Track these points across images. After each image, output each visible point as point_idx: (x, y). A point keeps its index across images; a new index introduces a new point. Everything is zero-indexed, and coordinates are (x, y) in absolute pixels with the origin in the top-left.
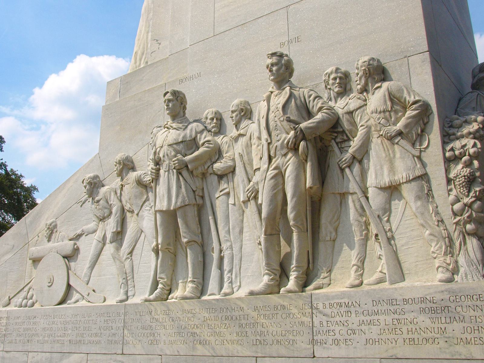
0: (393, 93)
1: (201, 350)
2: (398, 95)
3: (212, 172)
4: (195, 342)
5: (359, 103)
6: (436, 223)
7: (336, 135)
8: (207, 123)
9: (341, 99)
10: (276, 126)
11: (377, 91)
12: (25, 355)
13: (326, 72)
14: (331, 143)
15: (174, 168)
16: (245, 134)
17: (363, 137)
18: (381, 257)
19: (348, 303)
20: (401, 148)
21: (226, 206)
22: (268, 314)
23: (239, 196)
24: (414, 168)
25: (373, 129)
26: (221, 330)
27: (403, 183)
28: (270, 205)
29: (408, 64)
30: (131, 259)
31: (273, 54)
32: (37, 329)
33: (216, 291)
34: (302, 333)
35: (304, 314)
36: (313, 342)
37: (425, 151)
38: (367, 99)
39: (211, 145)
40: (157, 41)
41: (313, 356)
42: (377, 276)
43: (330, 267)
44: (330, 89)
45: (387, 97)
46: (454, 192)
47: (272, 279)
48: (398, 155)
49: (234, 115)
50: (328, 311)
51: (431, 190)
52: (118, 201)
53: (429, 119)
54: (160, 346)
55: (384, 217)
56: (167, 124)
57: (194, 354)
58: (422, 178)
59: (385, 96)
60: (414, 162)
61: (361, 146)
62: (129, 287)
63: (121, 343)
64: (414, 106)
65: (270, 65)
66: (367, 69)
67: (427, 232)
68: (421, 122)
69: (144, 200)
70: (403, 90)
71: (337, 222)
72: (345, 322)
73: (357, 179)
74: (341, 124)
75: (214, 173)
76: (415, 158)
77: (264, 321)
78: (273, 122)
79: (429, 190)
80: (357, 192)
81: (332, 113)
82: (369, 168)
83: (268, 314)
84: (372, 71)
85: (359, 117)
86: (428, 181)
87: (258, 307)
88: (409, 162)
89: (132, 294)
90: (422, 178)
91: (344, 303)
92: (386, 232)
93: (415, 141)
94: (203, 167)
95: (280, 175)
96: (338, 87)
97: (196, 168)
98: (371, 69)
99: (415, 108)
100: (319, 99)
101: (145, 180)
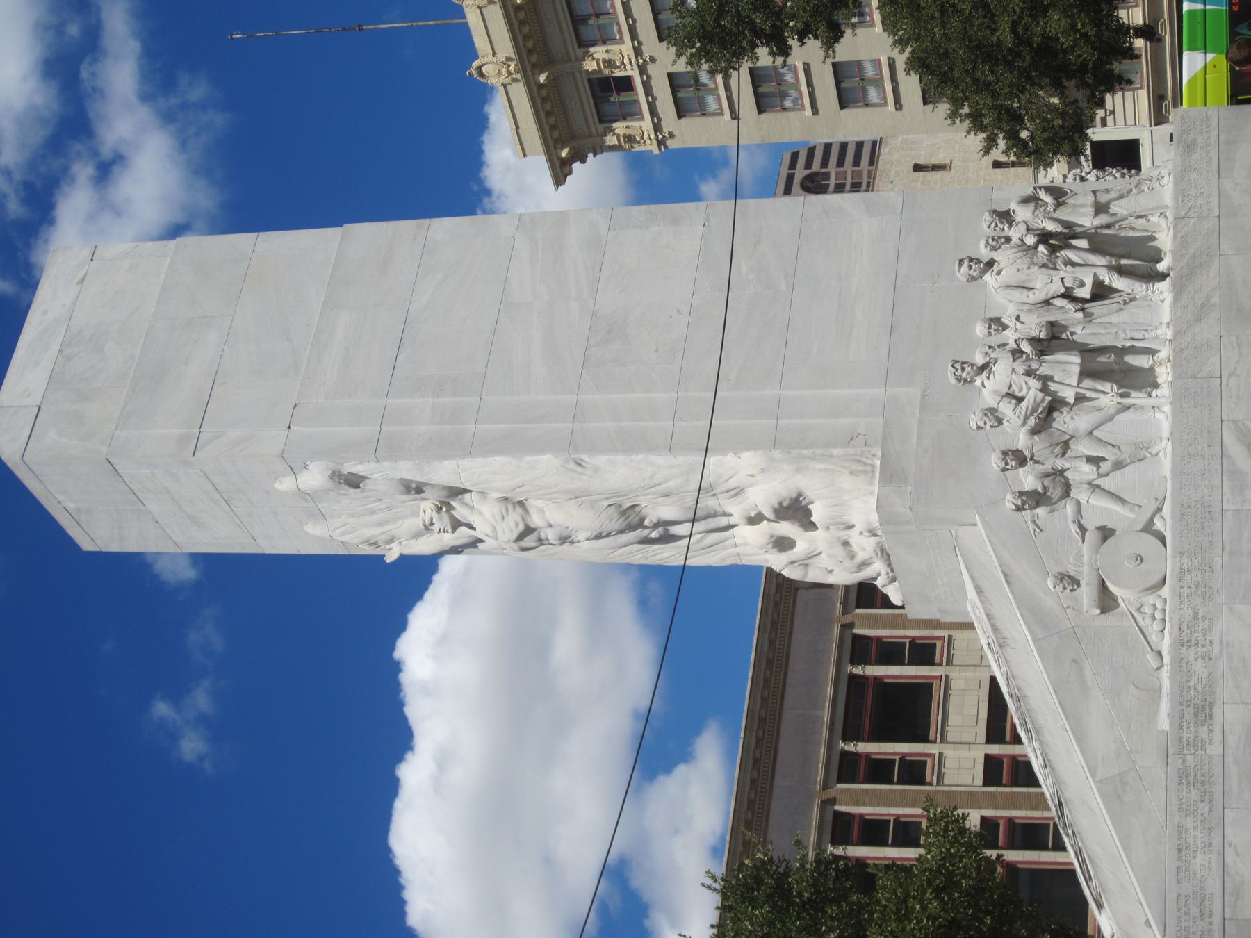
1: (1215, 300)
32: (1196, 499)
40: (852, 439)
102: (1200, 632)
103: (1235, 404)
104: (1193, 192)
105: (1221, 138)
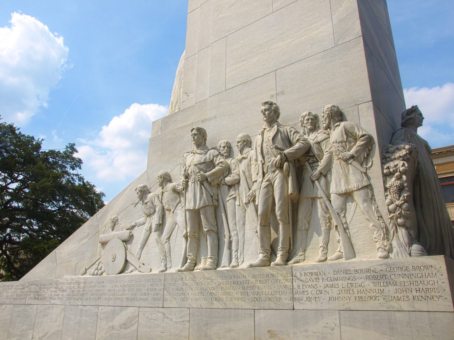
0: (347, 130)
1: (216, 304)
2: (351, 131)
3: (224, 183)
4: (213, 299)
5: (325, 136)
6: (377, 218)
7: (309, 158)
8: (221, 150)
9: (312, 133)
10: (268, 152)
11: (337, 128)
12: (97, 308)
13: (302, 115)
14: (305, 164)
15: (198, 181)
16: (247, 157)
17: (328, 159)
18: (339, 241)
19: (317, 273)
20: (353, 167)
21: (233, 206)
22: (262, 280)
23: (242, 199)
24: (362, 180)
25: (334, 154)
26: (231, 291)
27: (354, 191)
28: (263, 206)
29: (358, 109)
30: (169, 243)
31: (266, 103)
33: (227, 264)
34: (285, 293)
35: (287, 280)
36: (293, 299)
37: (369, 169)
38: (330, 133)
39: (223, 165)
41: (293, 309)
42: (337, 254)
43: (305, 248)
44: (305, 127)
45: (344, 132)
46: (389, 197)
47: (265, 256)
48: (351, 172)
49: (239, 144)
50: (303, 278)
51: (374, 196)
52: (160, 203)
53: (372, 147)
54: (188, 302)
55: (341, 214)
56: (193, 151)
57: (212, 307)
58: (367, 187)
59: (342, 131)
60: (362, 176)
61: (326, 166)
62: (168, 261)
63: (162, 300)
64: (362, 138)
65: (264, 111)
66: (330, 113)
67: (371, 224)
68: (367, 149)
69: (177, 202)
70: (354, 127)
71: (309, 218)
72: (315, 285)
73: (323, 188)
74: (312, 150)
75: (226, 184)
76: (363, 174)
77: (260, 285)
78: (266, 149)
79: (372, 196)
80: (323, 197)
81: (306, 143)
82: (331, 181)
83: (262, 280)
84: (333, 114)
85: (325, 146)
86: (372, 190)
87: (256, 275)
88: (359, 176)
89: (170, 267)
90: (367, 187)
91: (314, 273)
92: (343, 224)
93: (363, 162)
94: (218, 180)
95: (270, 186)
96: (310, 126)
97: (214, 181)
98: (333, 113)
99: (363, 139)
100: (297, 134)
101: (178, 188)
102: (59, 293)
103: (147, 317)
104: (321, 284)
105: (398, 314)
